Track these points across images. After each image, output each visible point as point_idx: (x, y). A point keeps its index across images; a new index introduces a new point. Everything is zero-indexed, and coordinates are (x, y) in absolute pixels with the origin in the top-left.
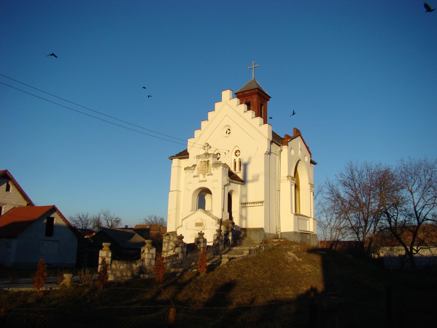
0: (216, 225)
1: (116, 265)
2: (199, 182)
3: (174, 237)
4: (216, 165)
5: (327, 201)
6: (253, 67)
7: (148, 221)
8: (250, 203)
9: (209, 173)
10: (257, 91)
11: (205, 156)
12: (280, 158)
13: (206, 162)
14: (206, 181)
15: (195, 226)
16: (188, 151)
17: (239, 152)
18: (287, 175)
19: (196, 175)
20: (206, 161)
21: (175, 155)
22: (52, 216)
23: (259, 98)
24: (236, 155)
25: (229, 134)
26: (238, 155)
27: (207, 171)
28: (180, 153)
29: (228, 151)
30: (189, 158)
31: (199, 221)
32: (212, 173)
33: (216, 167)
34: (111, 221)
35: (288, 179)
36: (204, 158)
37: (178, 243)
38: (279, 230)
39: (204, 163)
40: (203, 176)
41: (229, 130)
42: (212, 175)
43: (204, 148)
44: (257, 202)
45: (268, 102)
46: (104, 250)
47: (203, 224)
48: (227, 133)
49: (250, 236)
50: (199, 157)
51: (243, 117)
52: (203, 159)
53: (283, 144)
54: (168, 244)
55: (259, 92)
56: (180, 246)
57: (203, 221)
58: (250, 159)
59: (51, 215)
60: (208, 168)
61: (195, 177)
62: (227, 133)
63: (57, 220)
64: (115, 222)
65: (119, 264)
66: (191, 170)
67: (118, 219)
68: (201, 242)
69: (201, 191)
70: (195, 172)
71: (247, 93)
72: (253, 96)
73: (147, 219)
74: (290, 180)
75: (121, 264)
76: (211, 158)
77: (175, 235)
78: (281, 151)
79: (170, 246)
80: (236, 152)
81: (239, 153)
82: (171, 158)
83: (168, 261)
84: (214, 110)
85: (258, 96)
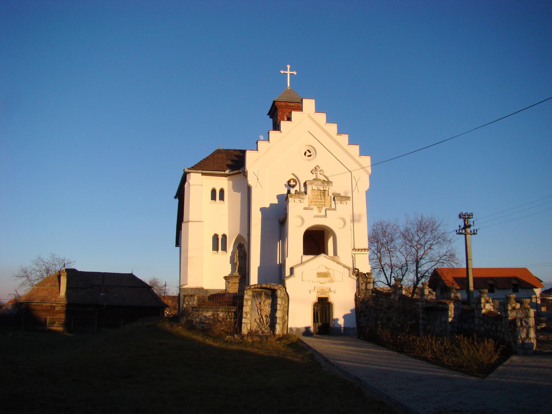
3: (281, 291)
4: (341, 198)
5: (419, 255)
9: (328, 207)
11: (321, 183)
19: (307, 207)
31: (324, 270)
36: (320, 185)
40: (318, 209)
42: (335, 209)
48: (310, 156)
51: (336, 141)
57: (329, 270)
60: (325, 199)
61: (305, 209)
66: (301, 199)
71: (292, 104)
84: (270, 118)
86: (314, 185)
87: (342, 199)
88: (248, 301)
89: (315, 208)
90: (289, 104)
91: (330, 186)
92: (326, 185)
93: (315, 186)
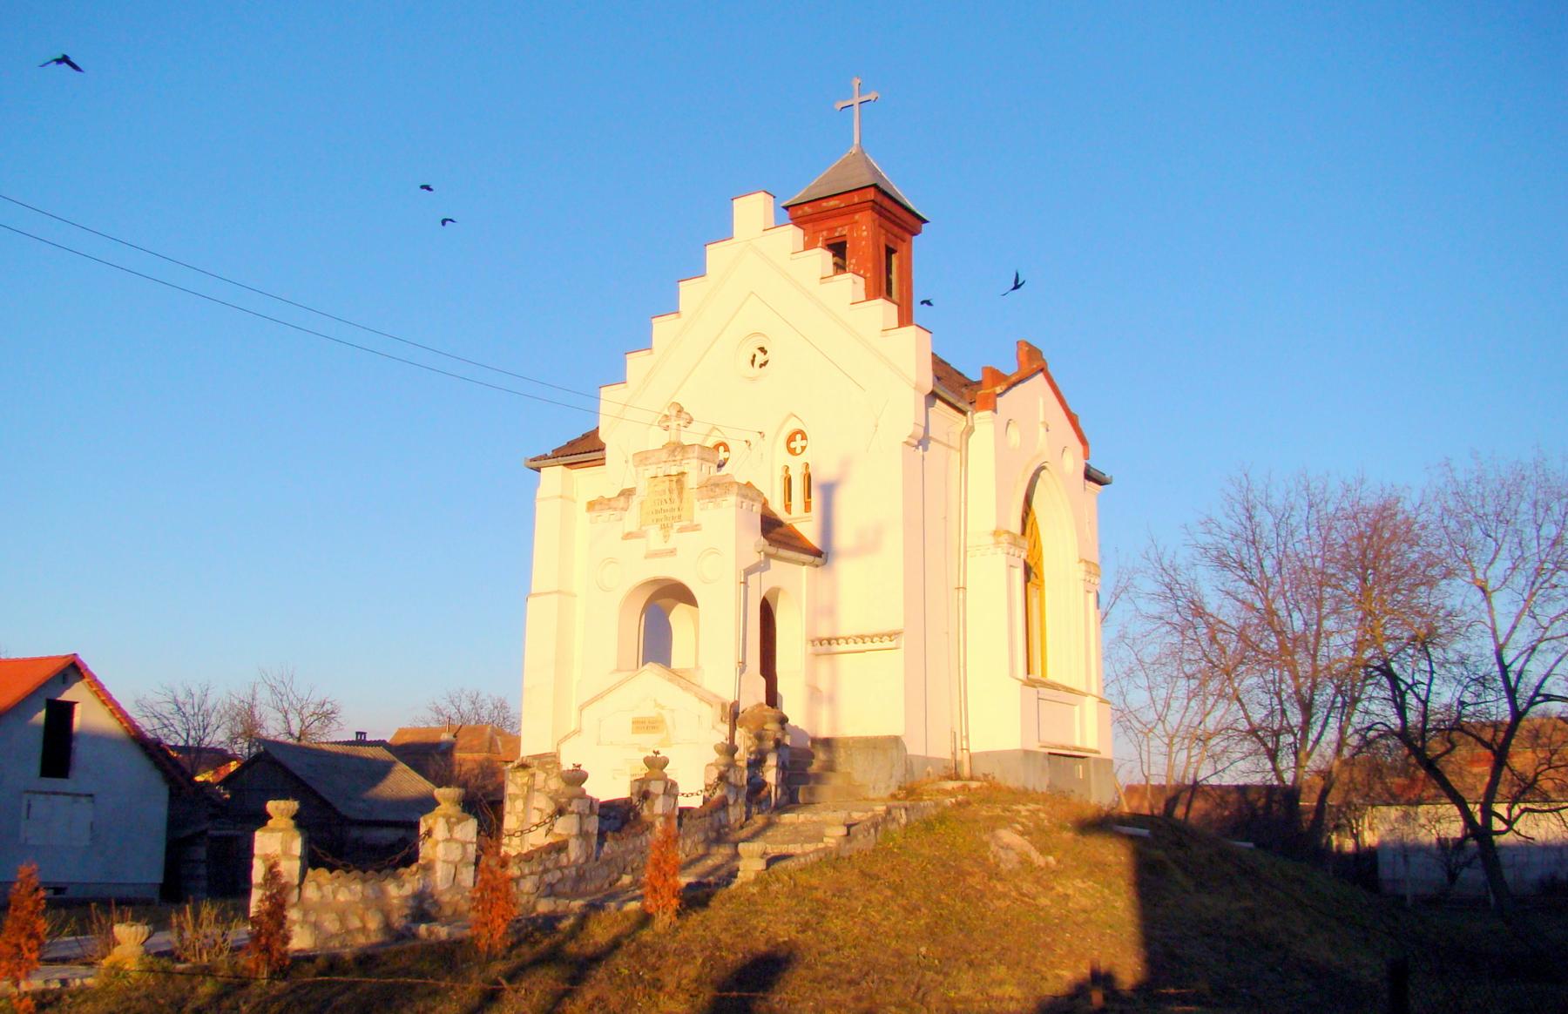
0: (713, 727)
1: (319, 887)
2: (646, 558)
3: (547, 773)
4: (712, 490)
5: (1153, 626)
6: (856, 101)
7: (444, 713)
8: (847, 640)
9: (685, 523)
10: (871, 194)
11: (667, 455)
12: (964, 462)
13: (674, 479)
14: (673, 552)
15: (633, 733)
16: (603, 436)
17: (804, 438)
18: (993, 527)
20: (672, 473)
21: (550, 454)
22: (67, 696)
23: (880, 226)
24: (792, 451)
25: (761, 366)
26: (798, 451)
27: (676, 513)
28: (571, 444)
29: (760, 433)
30: (604, 464)
31: (648, 711)
32: (695, 523)
33: (712, 498)
34: (300, 713)
35: (997, 544)
36: (665, 462)
37: (563, 800)
38: (964, 743)
39: (664, 482)
41: (762, 350)
42: (696, 528)
43: (665, 424)
44: (877, 635)
45: (914, 238)
46: (273, 830)
47: (662, 721)
48: (753, 362)
49: (849, 770)
50: (646, 458)
52: (660, 466)
53: (976, 404)
54: (524, 804)
55: (880, 198)
56: (572, 813)
58: (846, 464)
59: (62, 693)
61: (628, 536)
62: (753, 362)
63: (88, 715)
64: (315, 717)
65: (332, 884)
66: (615, 509)
67: (328, 707)
68: (658, 796)
69: (659, 590)
70: (631, 520)
71: (833, 203)
72: (857, 217)
73: (443, 704)
74: (1006, 545)
75: (340, 885)
76: (695, 463)
77: (553, 768)
78: (970, 431)
79: (536, 811)
80: (791, 439)
81: (804, 443)
82: (534, 464)
83: (526, 871)
85: (877, 216)
86: (650, 464)
87: (712, 494)
88: (515, 801)
89: (654, 534)
90: (825, 204)
91: (689, 458)
92: (679, 458)
93: (654, 466)
